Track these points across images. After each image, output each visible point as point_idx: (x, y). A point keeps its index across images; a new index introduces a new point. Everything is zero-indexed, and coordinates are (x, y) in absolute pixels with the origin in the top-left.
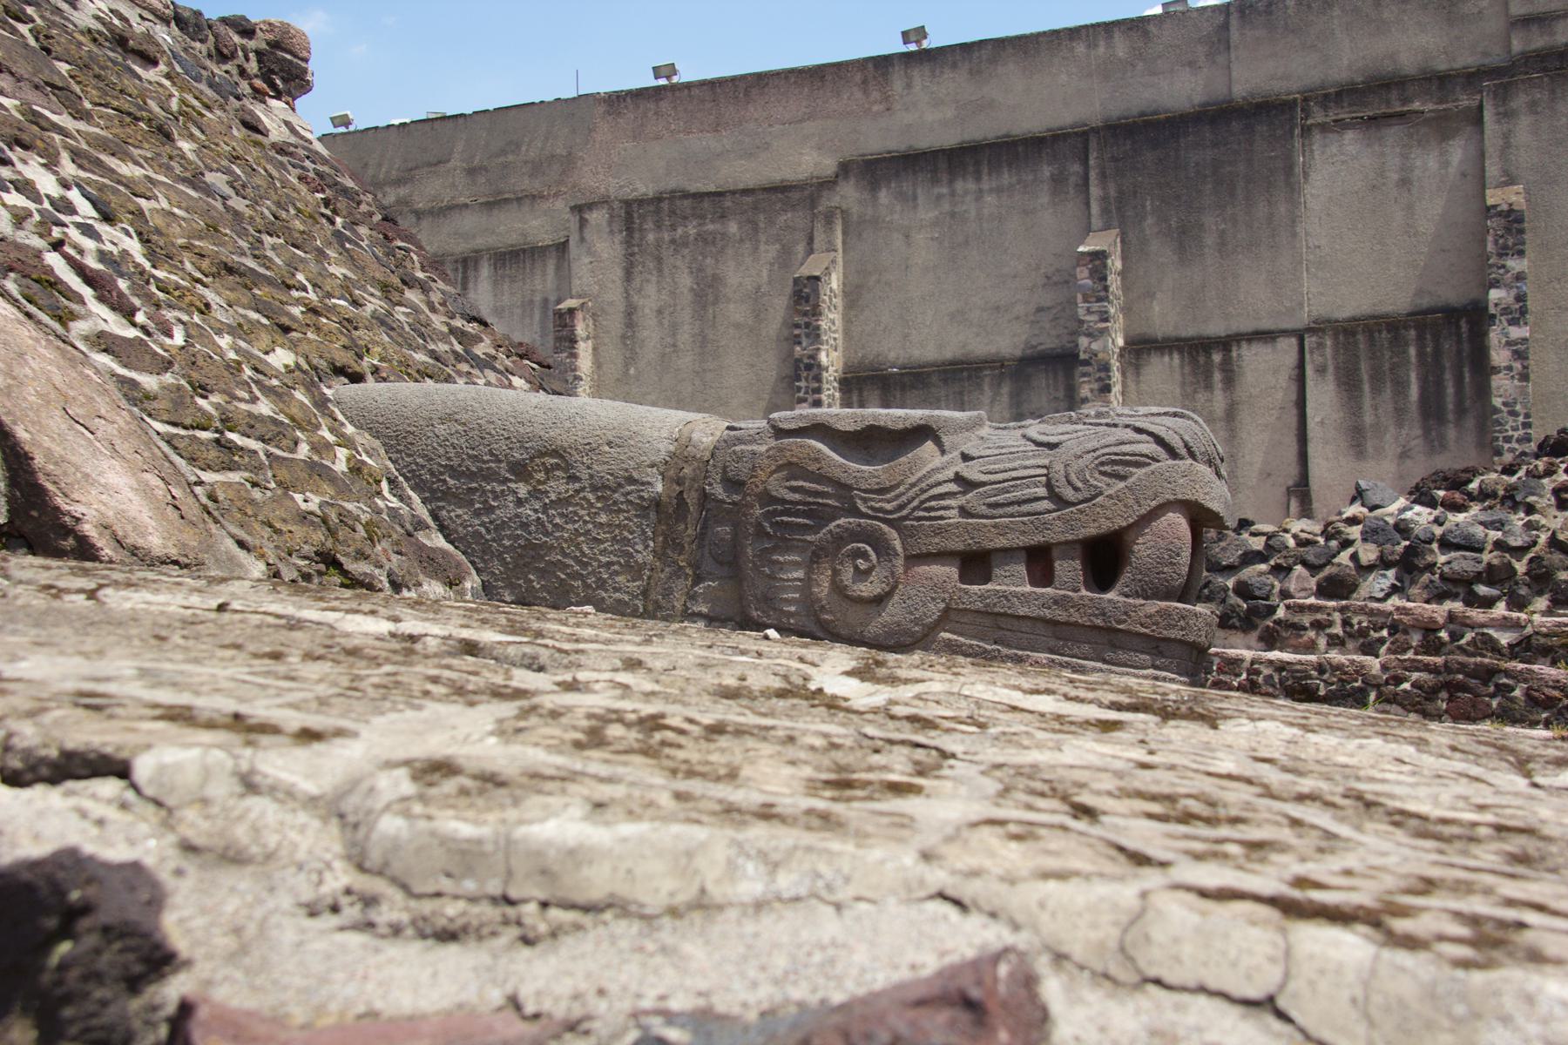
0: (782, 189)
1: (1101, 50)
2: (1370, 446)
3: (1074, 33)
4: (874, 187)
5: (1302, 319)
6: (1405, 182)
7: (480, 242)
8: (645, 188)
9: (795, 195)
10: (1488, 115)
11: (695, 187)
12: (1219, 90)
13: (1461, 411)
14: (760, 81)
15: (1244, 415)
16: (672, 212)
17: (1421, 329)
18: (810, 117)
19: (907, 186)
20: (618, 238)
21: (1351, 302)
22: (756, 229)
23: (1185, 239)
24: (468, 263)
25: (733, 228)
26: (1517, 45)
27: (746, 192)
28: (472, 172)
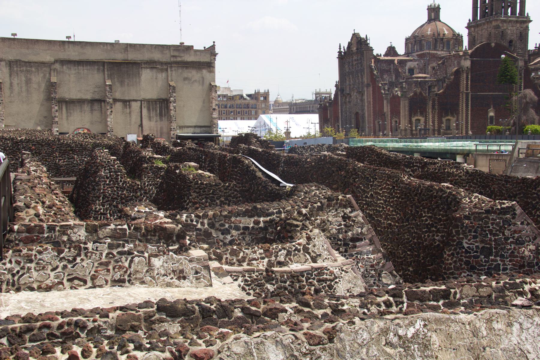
0: (43, 63)
1: (105, 47)
2: (152, 119)
3: (101, 43)
4: (63, 65)
5: (140, 98)
6: (156, 78)
9: (46, 65)
10: (169, 70)
11: (23, 59)
12: (126, 58)
13: (165, 115)
14: (37, 41)
15: (132, 113)
16: (20, 65)
17: (159, 102)
18: (49, 50)
19: (69, 66)
20: (8, 68)
22: (38, 70)
23: (122, 83)
25: (33, 69)
26: (172, 60)
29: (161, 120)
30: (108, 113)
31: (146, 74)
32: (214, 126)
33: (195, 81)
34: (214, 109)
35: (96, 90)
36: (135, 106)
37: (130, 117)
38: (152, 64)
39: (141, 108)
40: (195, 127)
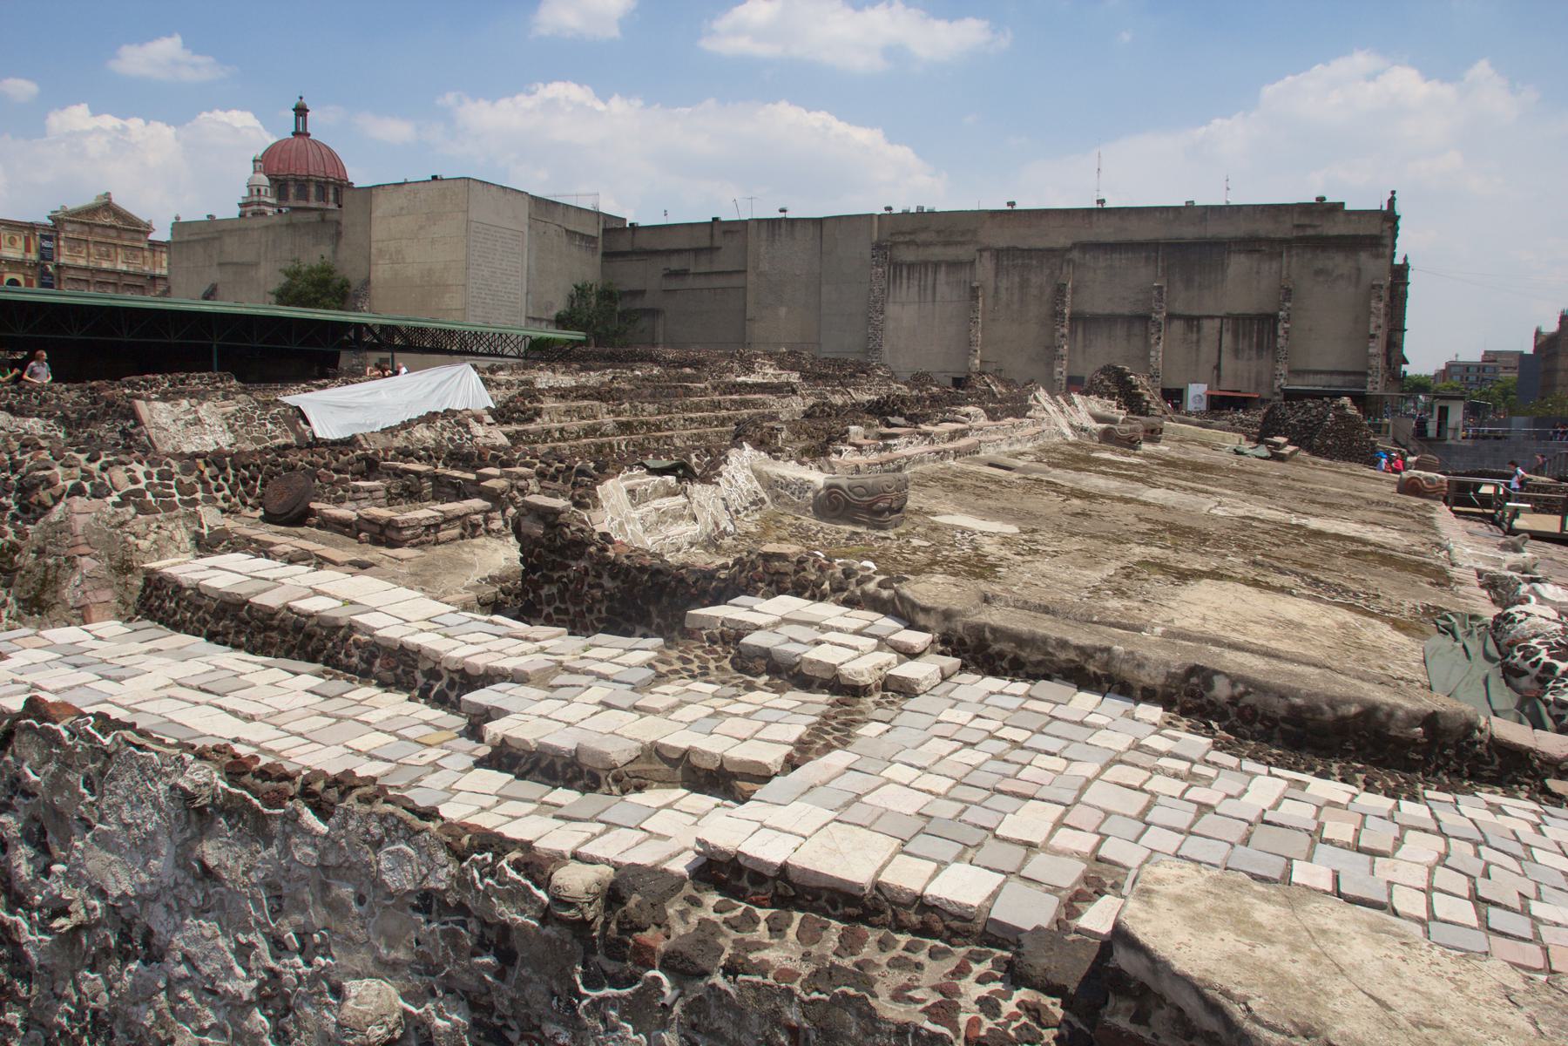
0: (1051, 250)
5: (1222, 313)
6: (1258, 273)
7: (941, 258)
8: (1001, 243)
11: (1020, 246)
13: (1268, 348)
20: (994, 262)
21: (1239, 309)
24: (937, 265)
25: (1034, 262)
27: (1040, 250)
28: (938, 232)
29: (1259, 356)
30: (1153, 341)
31: (1238, 265)
32: (1370, 372)
33: (1342, 276)
34: (1373, 336)
35: (1141, 297)
36: (1210, 327)
37: (1198, 350)
38: (1251, 245)
39: (1221, 333)
40: (1332, 373)
